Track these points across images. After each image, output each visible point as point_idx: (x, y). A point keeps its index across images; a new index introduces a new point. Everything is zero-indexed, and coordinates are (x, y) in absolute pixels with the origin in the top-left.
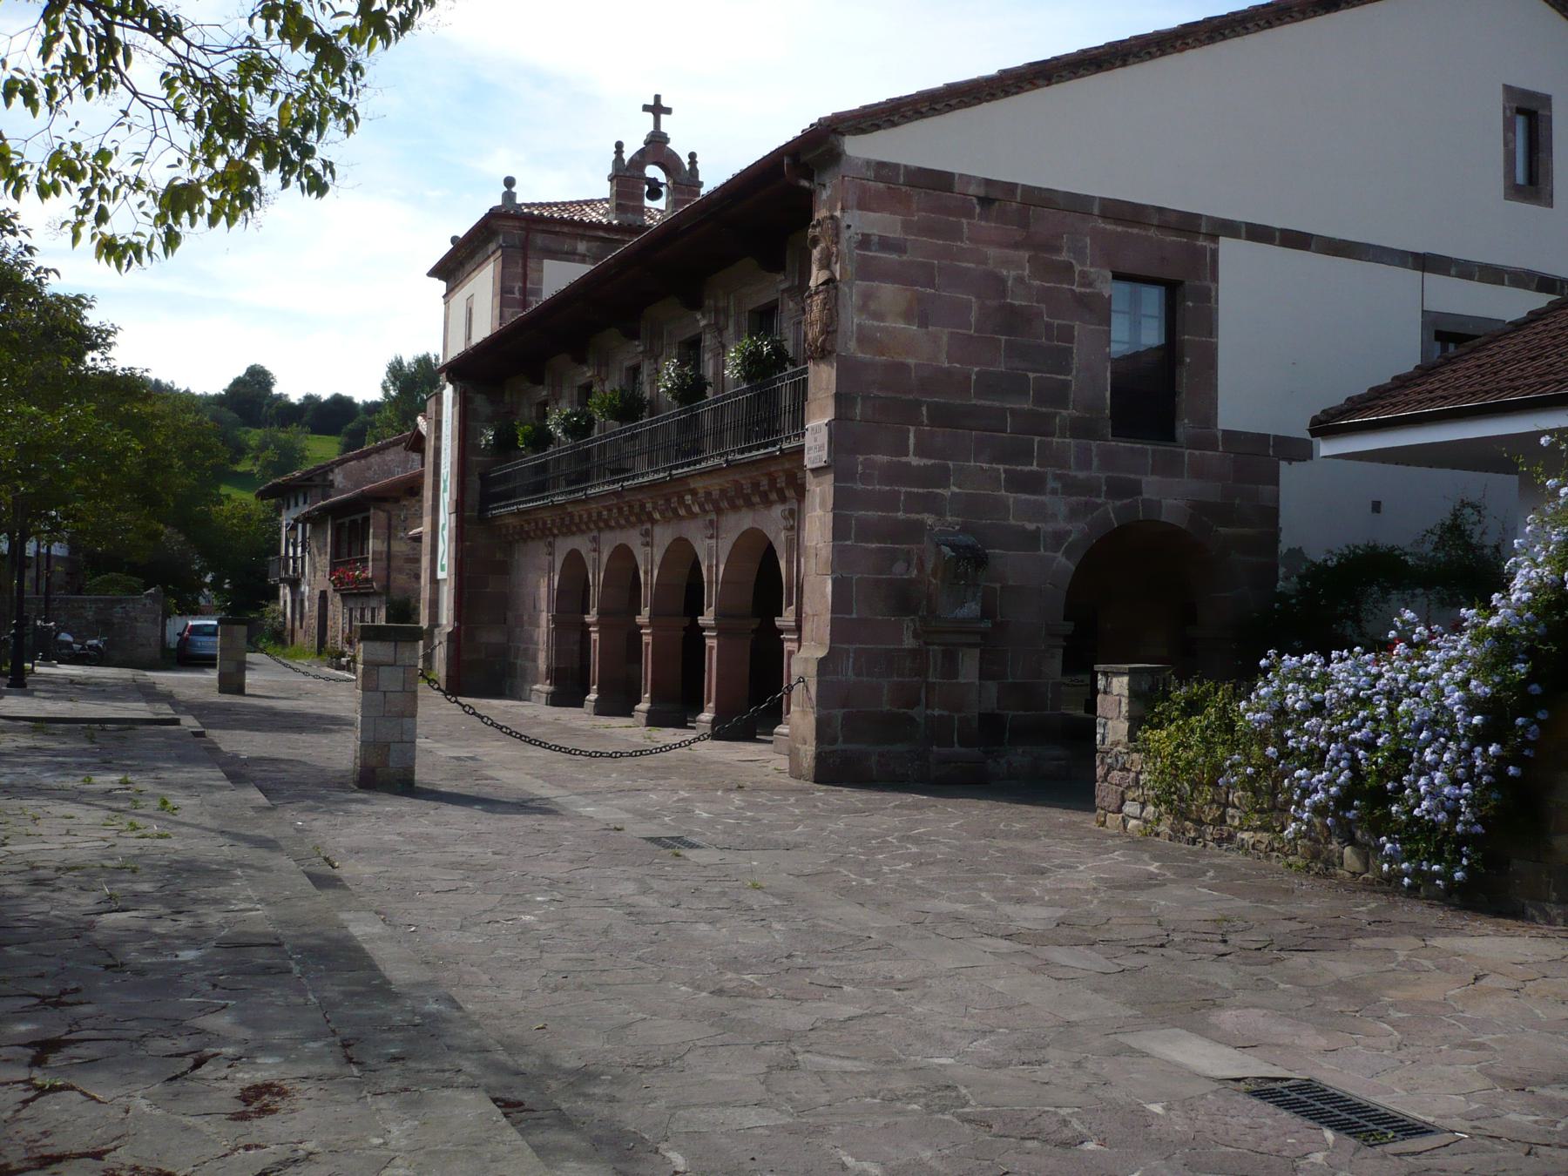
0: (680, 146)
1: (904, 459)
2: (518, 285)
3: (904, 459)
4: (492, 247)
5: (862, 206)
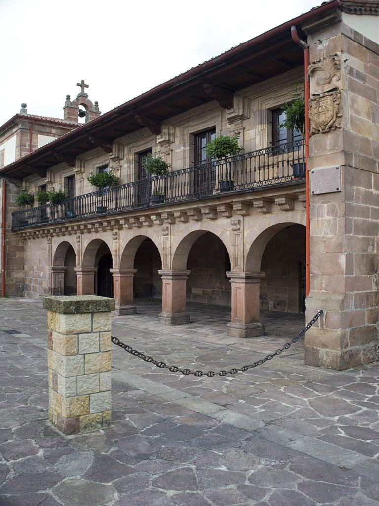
1: (370, 190)
3: (370, 190)
4: (14, 130)
5: (350, 53)
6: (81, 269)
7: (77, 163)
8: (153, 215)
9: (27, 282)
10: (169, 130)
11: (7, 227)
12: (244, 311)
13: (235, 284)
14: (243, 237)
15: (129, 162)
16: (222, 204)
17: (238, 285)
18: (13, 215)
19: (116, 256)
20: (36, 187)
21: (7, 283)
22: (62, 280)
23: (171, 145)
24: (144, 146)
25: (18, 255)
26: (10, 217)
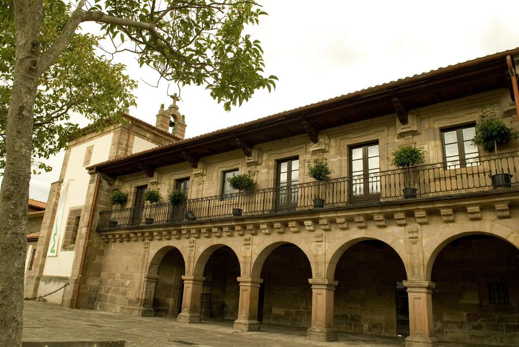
0: (181, 111)
2: (125, 142)
6: (192, 277)
7: (200, 165)
8: (307, 220)
9: (102, 292)
10: (325, 140)
11: (93, 226)
12: (427, 323)
13: (412, 294)
14: (422, 244)
15: (268, 167)
16: (401, 211)
17: (417, 295)
18: (100, 213)
19: (245, 263)
20: (131, 187)
21: (81, 291)
22: (153, 290)
23: (325, 154)
24: (288, 153)
25: (97, 260)
26: (98, 216)
